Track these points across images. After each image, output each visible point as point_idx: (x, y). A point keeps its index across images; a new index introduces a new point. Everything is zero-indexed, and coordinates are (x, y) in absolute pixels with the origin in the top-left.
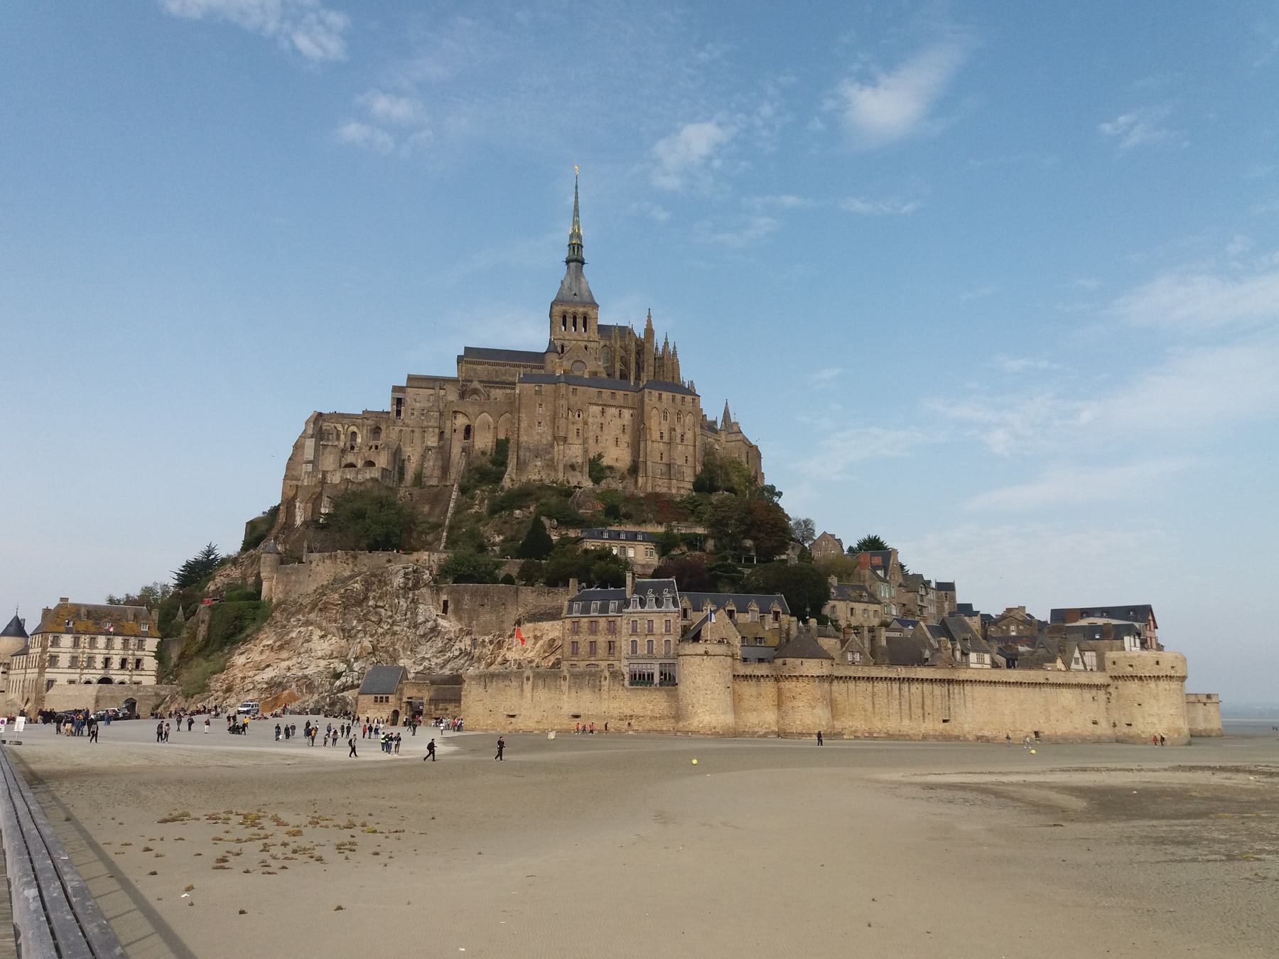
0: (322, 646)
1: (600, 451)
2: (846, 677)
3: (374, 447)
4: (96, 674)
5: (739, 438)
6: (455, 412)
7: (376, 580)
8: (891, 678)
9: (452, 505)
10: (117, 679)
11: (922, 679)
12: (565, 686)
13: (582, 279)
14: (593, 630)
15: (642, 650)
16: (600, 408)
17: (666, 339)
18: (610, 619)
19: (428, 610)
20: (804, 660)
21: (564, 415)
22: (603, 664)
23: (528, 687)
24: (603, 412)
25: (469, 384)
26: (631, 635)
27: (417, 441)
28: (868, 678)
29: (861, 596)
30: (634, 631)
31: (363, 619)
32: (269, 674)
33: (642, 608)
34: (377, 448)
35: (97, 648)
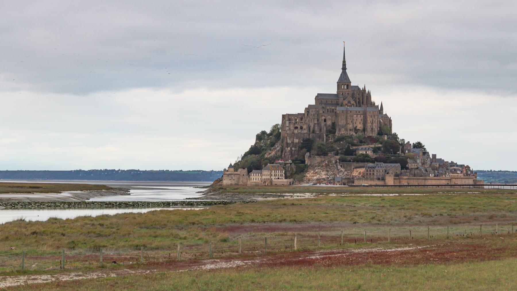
0: (323, 173)
1: (356, 125)
4: (277, 177)
7: (330, 162)
9: (325, 139)
10: (280, 178)
12: (369, 180)
14: (370, 171)
15: (378, 174)
19: (339, 167)
22: (372, 177)
23: (364, 180)
24: (357, 116)
27: (313, 122)
30: (377, 171)
31: (330, 168)
32: (315, 178)
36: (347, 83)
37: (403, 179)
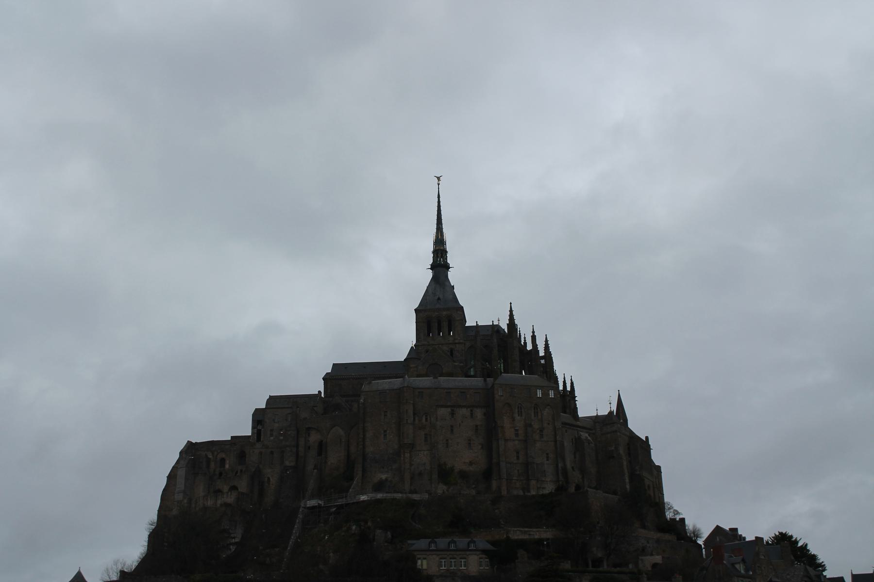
6: (309, 429)
16: (449, 410)
17: (533, 332)
21: (409, 422)
24: (453, 414)
25: (331, 399)
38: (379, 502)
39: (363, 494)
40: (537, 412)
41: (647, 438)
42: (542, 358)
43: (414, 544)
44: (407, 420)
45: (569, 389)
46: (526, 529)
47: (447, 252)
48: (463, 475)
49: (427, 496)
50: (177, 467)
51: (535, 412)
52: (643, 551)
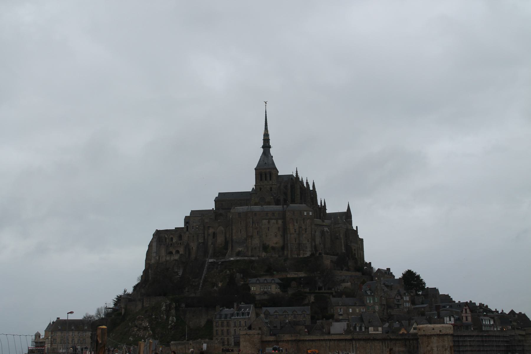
2: (304, 340)
3: (179, 244)
5: (339, 226)
6: (209, 227)
8: (321, 339)
11: (334, 339)
13: (269, 155)
16: (267, 220)
17: (307, 180)
18: (228, 321)
20: (284, 334)
22: (226, 338)
24: (269, 222)
26: (234, 327)
28: (312, 340)
29: (356, 303)
33: (238, 317)
34: (180, 243)
35: (69, 336)
36: (268, 170)
37: (283, 341)
38: (238, 261)
39: (232, 257)
40: (304, 222)
41: (357, 227)
42: (312, 190)
43: (251, 281)
44: (250, 226)
45: (323, 205)
46: (296, 273)
47: (269, 140)
48: (273, 248)
49: (258, 258)
50: (152, 242)
51: (303, 222)
52: (344, 281)
